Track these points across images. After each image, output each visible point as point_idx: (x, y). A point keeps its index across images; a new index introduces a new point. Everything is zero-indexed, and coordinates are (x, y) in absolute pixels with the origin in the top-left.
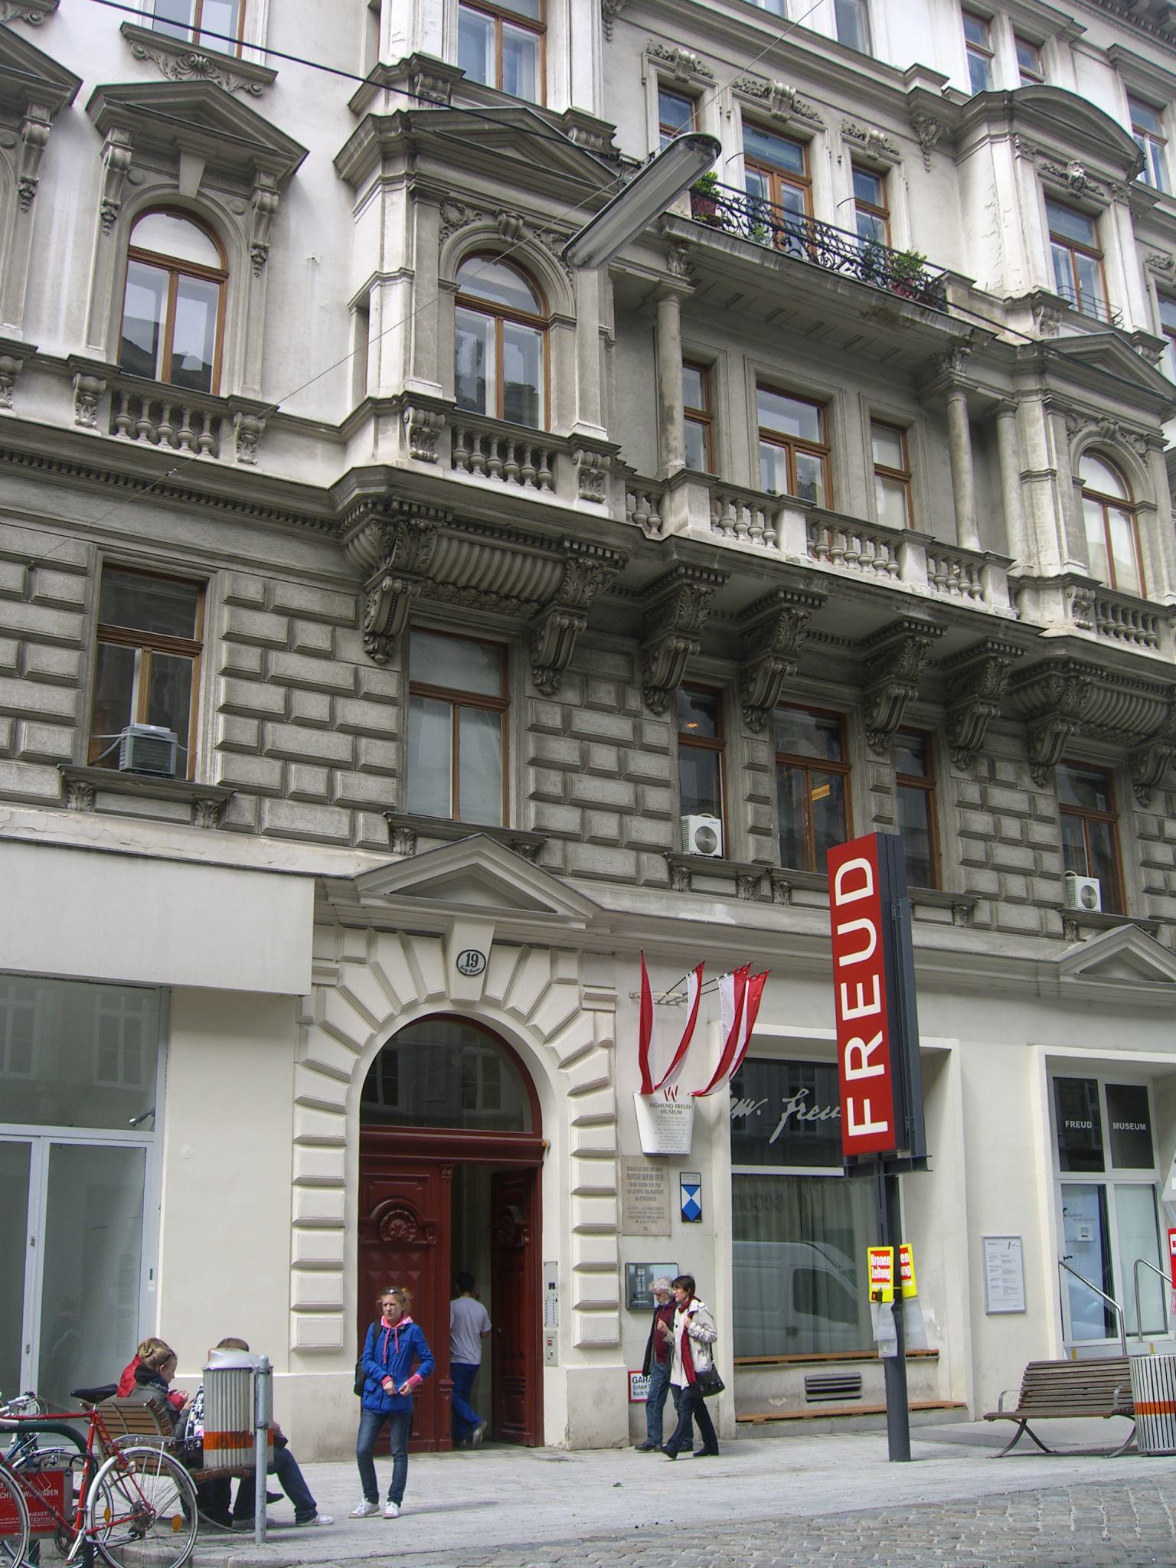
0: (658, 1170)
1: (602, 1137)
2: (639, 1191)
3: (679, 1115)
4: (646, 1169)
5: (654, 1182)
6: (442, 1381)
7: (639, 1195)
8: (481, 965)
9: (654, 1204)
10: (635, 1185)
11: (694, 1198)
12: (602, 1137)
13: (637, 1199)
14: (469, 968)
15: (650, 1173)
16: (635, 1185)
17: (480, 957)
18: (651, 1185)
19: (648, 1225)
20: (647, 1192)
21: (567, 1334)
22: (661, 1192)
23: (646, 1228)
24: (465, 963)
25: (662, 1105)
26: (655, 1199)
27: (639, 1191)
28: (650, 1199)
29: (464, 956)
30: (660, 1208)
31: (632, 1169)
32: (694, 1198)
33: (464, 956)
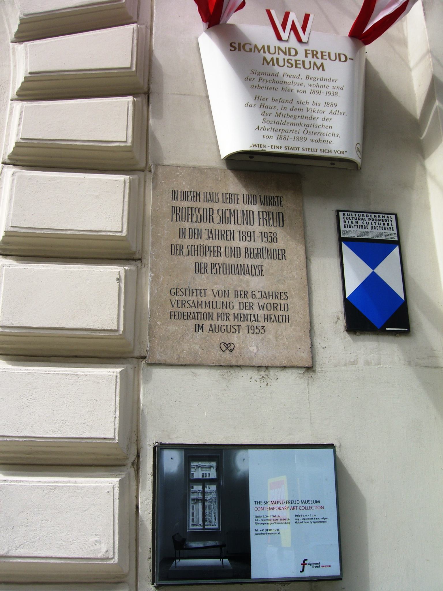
0: (267, 201)
2: (206, 250)
3: (314, 73)
4: (232, 198)
7: (207, 260)
10: (196, 234)
11: (382, 271)
13: (200, 268)
15: (242, 207)
16: (196, 234)
18: (245, 236)
19: (234, 338)
20: (235, 252)
22: (280, 255)
23: (228, 347)
25: (266, 49)
26: (260, 271)
27: (206, 250)
28: (241, 270)
30: (276, 295)
31: (185, 196)
32: (382, 271)
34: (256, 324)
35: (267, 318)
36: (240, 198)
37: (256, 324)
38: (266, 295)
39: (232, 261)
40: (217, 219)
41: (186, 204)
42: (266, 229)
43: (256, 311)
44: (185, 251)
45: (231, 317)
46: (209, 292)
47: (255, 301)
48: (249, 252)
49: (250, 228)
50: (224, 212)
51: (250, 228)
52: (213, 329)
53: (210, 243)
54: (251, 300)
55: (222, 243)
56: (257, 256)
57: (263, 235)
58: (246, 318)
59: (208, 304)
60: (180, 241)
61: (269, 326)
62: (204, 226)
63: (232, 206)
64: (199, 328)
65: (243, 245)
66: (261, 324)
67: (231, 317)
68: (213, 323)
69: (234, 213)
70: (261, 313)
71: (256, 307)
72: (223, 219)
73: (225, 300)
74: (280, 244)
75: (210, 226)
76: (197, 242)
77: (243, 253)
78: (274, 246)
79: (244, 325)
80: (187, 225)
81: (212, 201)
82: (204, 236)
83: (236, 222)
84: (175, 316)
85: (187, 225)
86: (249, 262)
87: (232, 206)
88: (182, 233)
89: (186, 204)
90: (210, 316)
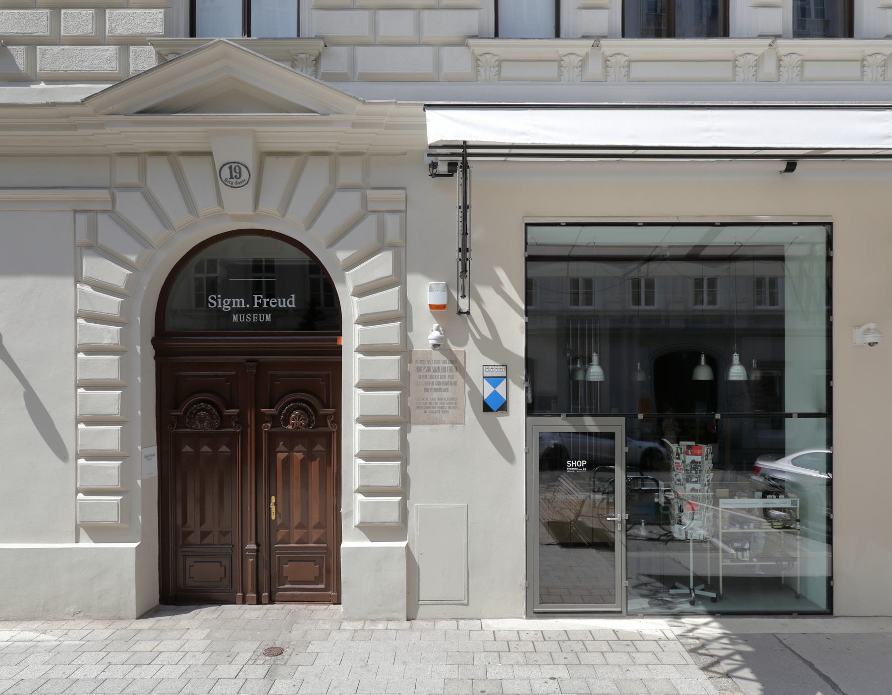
1: (390, 333)
4: (438, 362)
5: (447, 374)
6: (248, 547)
7: (429, 387)
8: (245, 175)
9: (445, 395)
10: (425, 377)
12: (390, 333)
13: (426, 390)
14: (234, 181)
16: (425, 377)
17: (244, 169)
20: (439, 383)
21: (350, 513)
22: (455, 383)
24: (228, 176)
26: (447, 390)
28: (440, 390)
29: (226, 168)
30: (452, 399)
31: (420, 362)
33: (226, 168)
34: (445, 410)
35: (449, 408)
36: (441, 361)
37: (445, 410)
38: (449, 399)
39: (437, 387)
40: (432, 371)
41: (421, 365)
42: (450, 374)
43: (446, 405)
44: (421, 384)
45: (437, 408)
46: (429, 399)
47: (445, 402)
48: (443, 383)
49: (444, 374)
50: (435, 368)
51: (444, 374)
52: (431, 412)
53: (429, 380)
54: (444, 401)
55: (434, 380)
56: (446, 385)
57: (449, 376)
58: (442, 408)
59: (429, 403)
60: (419, 380)
61: (451, 411)
62: (427, 374)
63: (438, 365)
64: (426, 412)
65: (441, 380)
66: (447, 410)
67: (437, 408)
68: (430, 410)
69: (438, 368)
70: (447, 406)
71: (445, 404)
72: (435, 371)
73: (435, 401)
74: (455, 380)
75: (429, 374)
76: (426, 380)
77: (441, 384)
78: (453, 380)
79: (441, 410)
80: (421, 374)
81: (430, 363)
82: (428, 378)
83: (439, 372)
84: (417, 408)
85: (421, 374)
86: (444, 387)
87: (438, 365)
88: (420, 377)
89: (421, 365)
90: (430, 408)
